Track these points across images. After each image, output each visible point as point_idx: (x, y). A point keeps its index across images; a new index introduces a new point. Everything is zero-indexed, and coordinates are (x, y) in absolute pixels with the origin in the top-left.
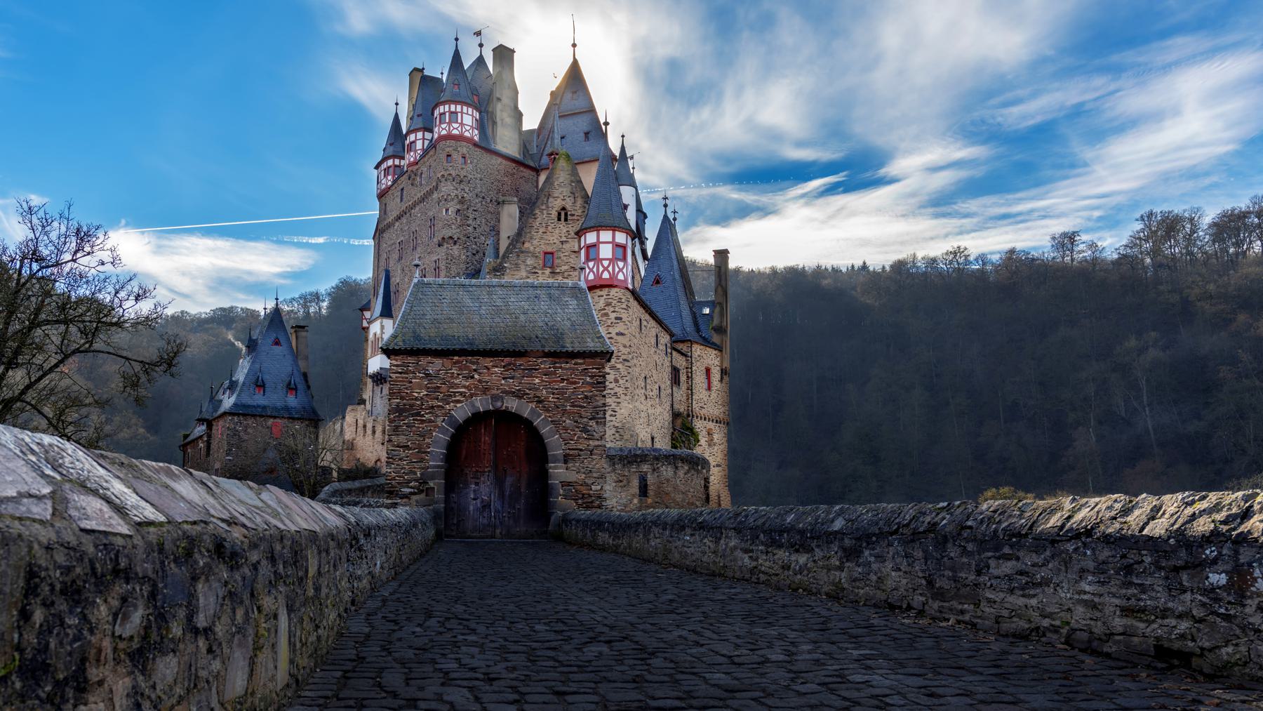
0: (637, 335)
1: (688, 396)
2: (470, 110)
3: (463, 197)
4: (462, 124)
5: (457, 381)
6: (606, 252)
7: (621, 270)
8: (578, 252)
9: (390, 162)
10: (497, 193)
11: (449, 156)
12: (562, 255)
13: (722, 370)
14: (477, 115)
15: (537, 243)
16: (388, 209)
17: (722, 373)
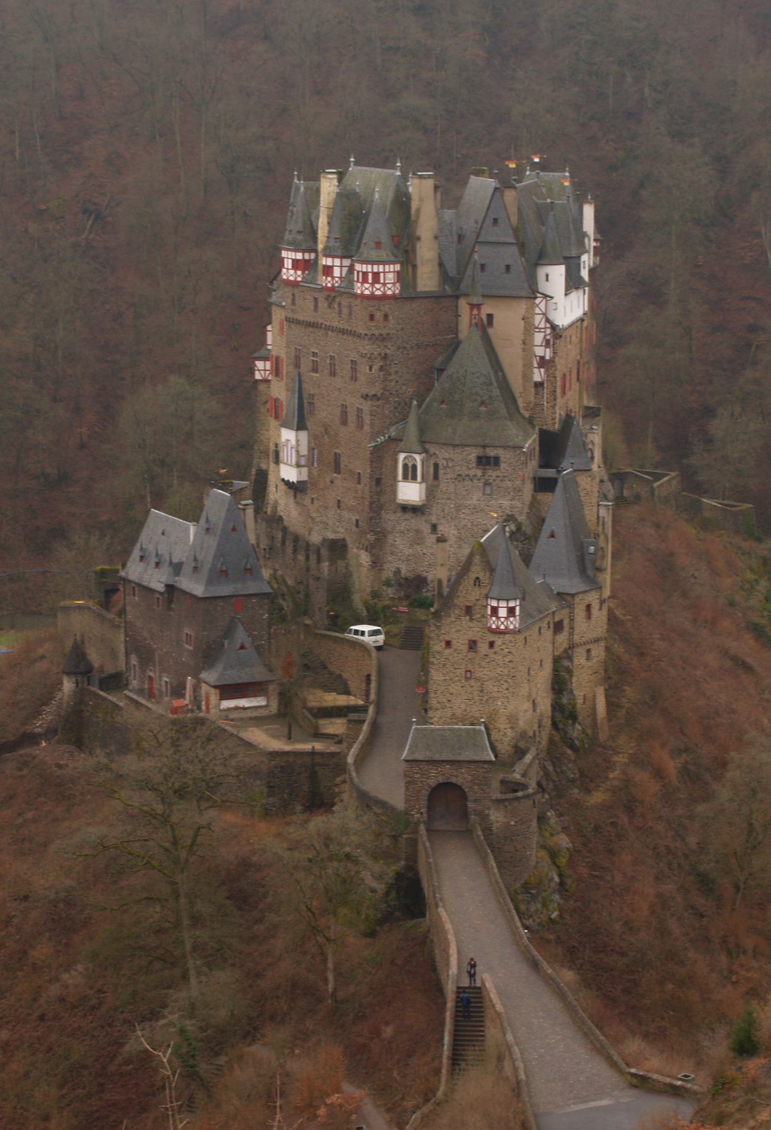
3: (386, 354)
4: (384, 284)
6: (503, 613)
8: (486, 607)
9: (299, 256)
11: (372, 317)
14: (398, 267)
15: (461, 601)
16: (296, 302)
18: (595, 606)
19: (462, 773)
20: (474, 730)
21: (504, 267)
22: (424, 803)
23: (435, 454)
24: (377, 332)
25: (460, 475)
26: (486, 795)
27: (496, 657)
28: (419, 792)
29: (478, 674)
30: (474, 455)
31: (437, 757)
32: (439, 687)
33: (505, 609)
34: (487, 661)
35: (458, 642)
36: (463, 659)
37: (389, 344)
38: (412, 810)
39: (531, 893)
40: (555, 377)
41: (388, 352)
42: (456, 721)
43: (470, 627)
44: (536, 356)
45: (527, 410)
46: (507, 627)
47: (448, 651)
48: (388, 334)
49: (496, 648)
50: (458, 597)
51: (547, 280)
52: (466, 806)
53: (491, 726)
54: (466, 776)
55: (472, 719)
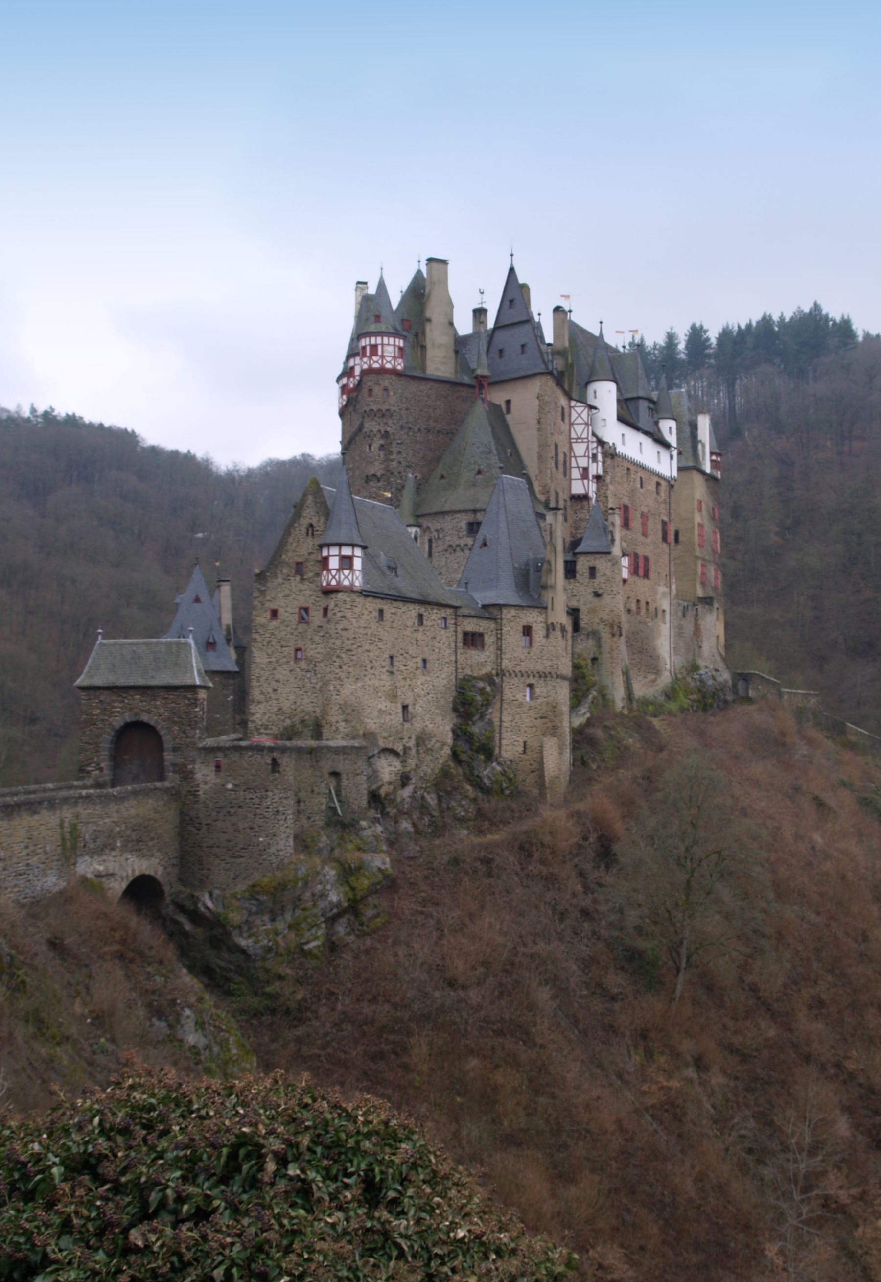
0: (374, 625)
1: (497, 656)
2: (392, 340)
3: (386, 432)
4: (383, 357)
5: (116, 704)
6: (334, 563)
7: (346, 577)
10: (427, 421)
12: (308, 564)
13: (547, 626)
14: (400, 343)
15: (289, 557)
17: (548, 629)
18: (539, 632)
19: (156, 707)
20: (178, 644)
21: (519, 347)
22: (105, 754)
23: (428, 528)
24: (375, 408)
25: (450, 546)
26: (189, 740)
27: (329, 627)
28: (98, 736)
29: (310, 653)
30: (465, 522)
31: (122, 682)
32: (262, 672)
33: (337, 558)
34: (321, 634)
35: (286, 611)
36: (292, 634)
37: (390, 422)
38: (89, 765)
39: (257, 900)
40: (607, 497)
41: (388, 429)
42: (282, 718)
43: (301, 591)
44: (578, 467)
45: (543, 494)
46: (339, 582)
47: (274, 623)
48: (388, 410)
49: (330, 613)
50: (287, 551)
51: (595, 397)
52: (162, 759)
53: (324, 722)
54: (162, 710)
55: (302, 715)
